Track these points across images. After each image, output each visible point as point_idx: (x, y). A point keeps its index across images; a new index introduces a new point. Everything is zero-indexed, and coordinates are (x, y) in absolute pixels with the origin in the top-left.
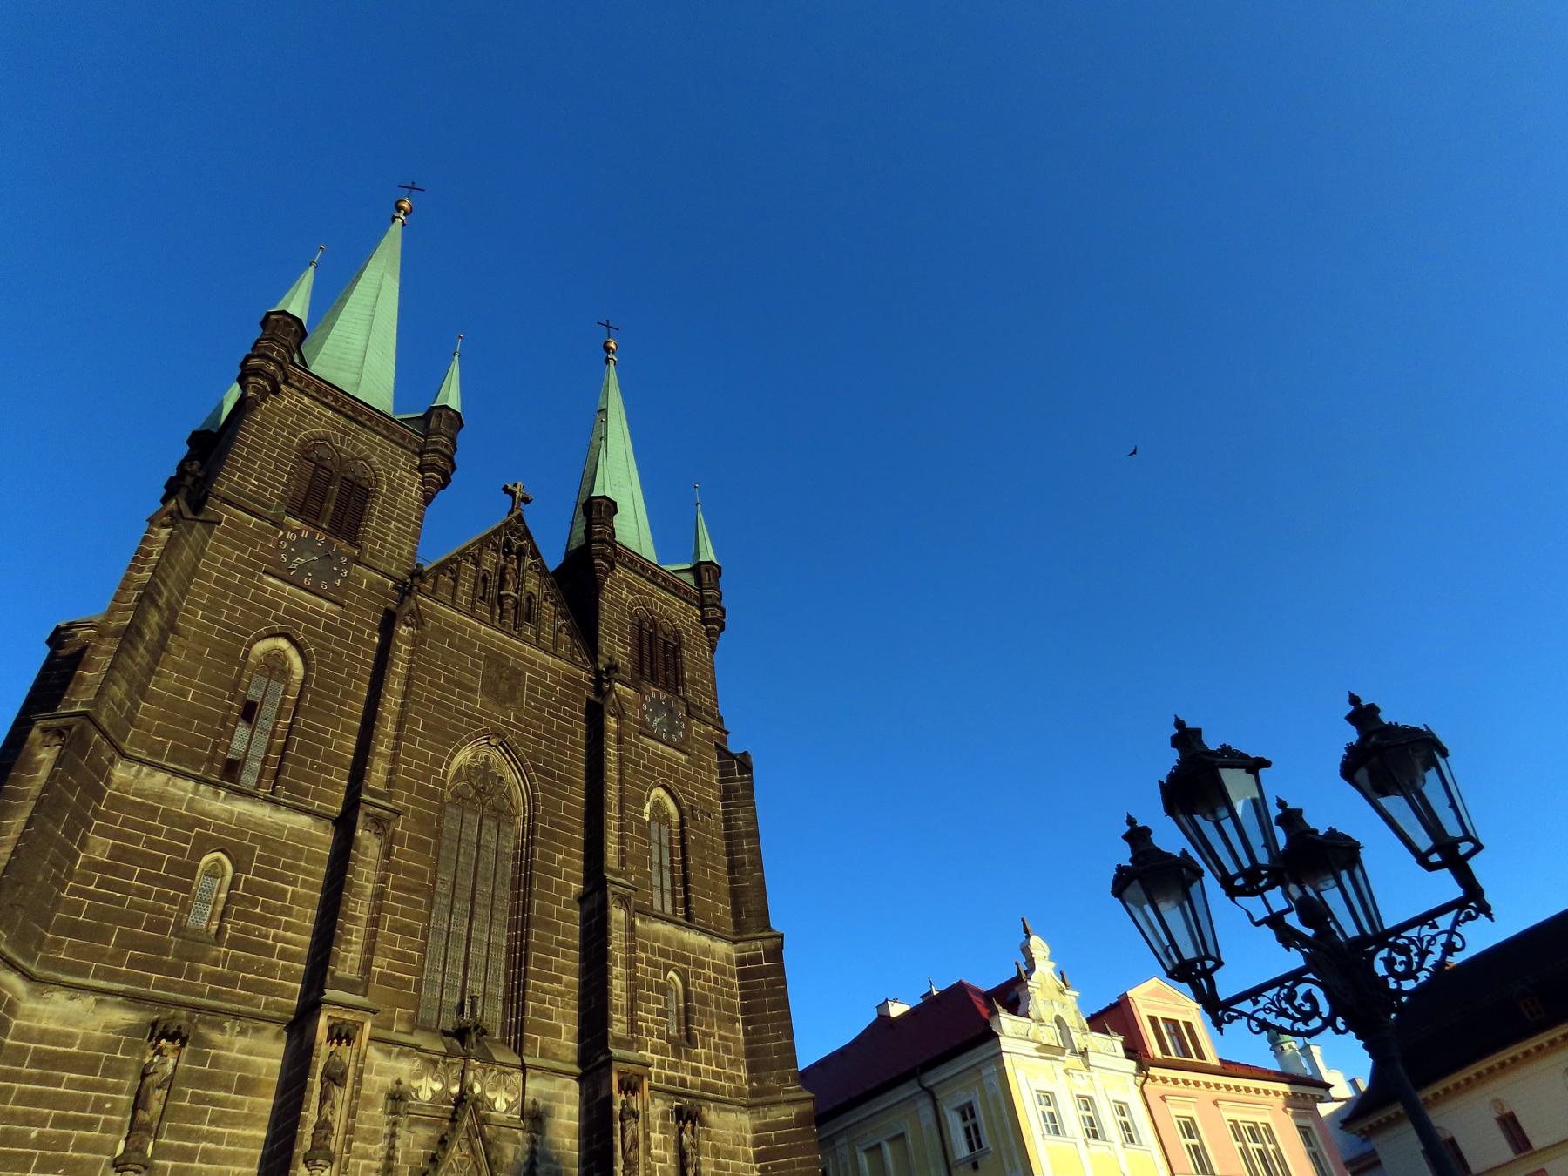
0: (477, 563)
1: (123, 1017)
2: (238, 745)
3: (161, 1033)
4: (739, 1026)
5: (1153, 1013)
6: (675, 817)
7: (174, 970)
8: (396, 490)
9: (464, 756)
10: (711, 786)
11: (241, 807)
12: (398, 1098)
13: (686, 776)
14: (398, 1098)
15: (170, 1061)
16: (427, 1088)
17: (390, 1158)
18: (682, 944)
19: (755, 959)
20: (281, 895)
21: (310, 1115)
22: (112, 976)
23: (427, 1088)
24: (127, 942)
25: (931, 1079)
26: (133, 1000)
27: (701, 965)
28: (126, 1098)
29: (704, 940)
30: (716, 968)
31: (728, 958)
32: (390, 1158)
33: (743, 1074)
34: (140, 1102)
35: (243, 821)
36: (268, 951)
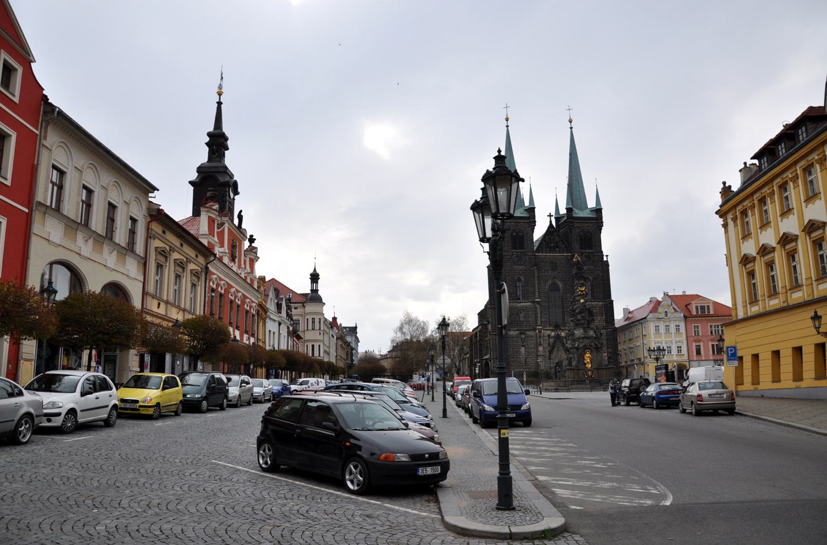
0: (545, 241)
1: (517, 332)
2: (518, 294)
3: (521, 334)
4: (604, 316)
5: (697, 305)
6: (592, 280)
7: (521, 326)
8: (527, 234)
9: (550, 282)
10: (599, 270)
11: (522, 304)
12: (549, 336)
13: (593, 270)
14: (549, 336)
15: (523, 336)
16: (553, 334)
17: (549, 342)
18: (592, 305)
19: (607, 305)
20: (529, 314)
21: (538, 341)
22: (515, 328)
23: (553, 334)
24: (515, 324)
25: (641, 321)
26: (517, 330)
27: (596, 307)
28: (520, 340)
29: (597, 303)
30: (599, 307)
31: (602, 305)
32: (549, 342)
33: (604, 324)
34: (522, 340)
35: (522, 306)
36: (530, 321)
